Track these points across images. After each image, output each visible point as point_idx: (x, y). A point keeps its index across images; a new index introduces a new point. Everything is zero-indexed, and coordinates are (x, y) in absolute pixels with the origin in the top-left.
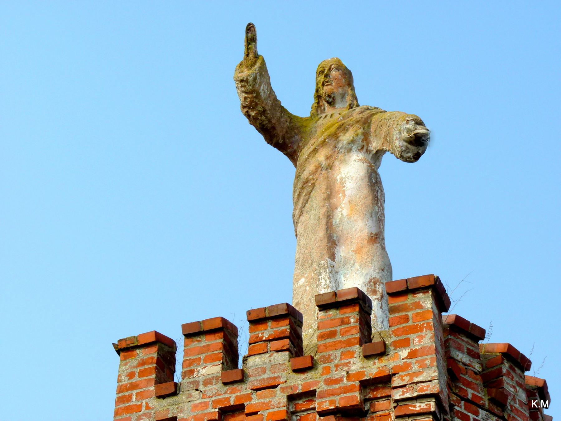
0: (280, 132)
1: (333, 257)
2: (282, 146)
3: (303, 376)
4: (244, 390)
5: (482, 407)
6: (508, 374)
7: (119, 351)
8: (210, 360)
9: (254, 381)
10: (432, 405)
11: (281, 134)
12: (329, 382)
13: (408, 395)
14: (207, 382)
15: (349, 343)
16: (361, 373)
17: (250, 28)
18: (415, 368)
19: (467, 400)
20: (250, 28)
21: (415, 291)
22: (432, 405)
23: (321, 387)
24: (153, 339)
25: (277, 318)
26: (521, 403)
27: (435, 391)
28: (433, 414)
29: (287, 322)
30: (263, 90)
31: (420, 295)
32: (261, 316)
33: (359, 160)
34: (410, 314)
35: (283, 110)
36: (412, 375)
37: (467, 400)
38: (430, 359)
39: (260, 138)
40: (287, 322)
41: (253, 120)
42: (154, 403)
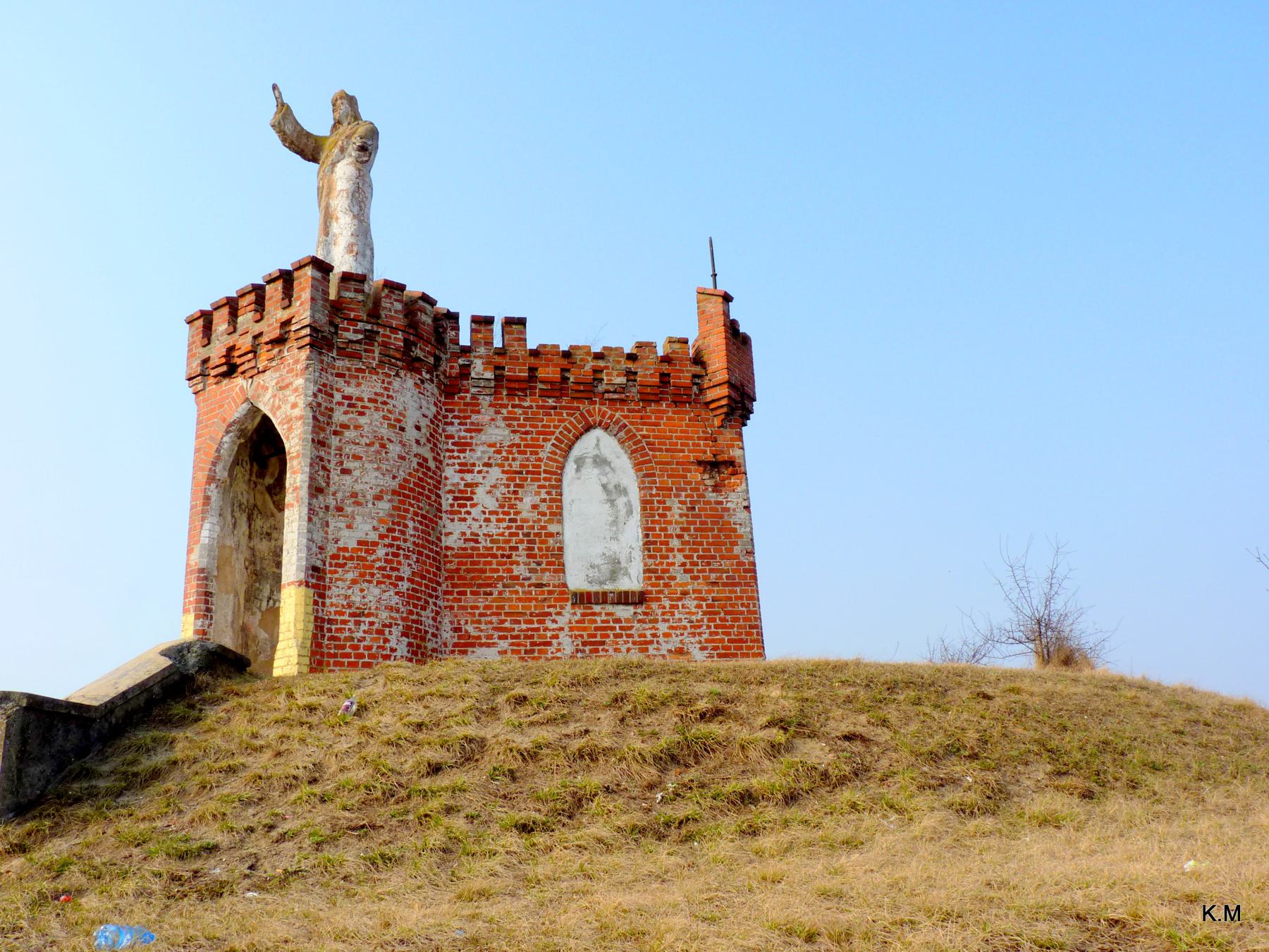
0: (308, 152)
1: (327, 234)
2: (314, 159)
3: (259, 324)
4: (236, 336)
5: (361, 321)
6: (387, 296)
7: (188, 323)
8: (223, 322)
9: (240, 330)
10: (307, 331)
11: (309, 153)
12: (269, 325)
13: (298, 328)
14: (222, 335)
15: (277, 302)
16: (281, 319)
17: (275, 87)
18: (301, 311)
19: (349, 320)
20: (275, 87)
21: (305, 266)
22: (307, 331)
23: (265, 329)
24: (199, 314)
25: (249, 292)
26: (396, 312)
27: (308, 323)
28: (310, 335)
29: (254, 294)
30: (288, 128)
31: (307, 268)
32: (242, 293)
33: (351, 163)
34: (302, 280)
35: (309, 135)
36: (302, 315)
37: (349, 320)
38: (308, 306)
39: (298, 157)
40: (254, 294)
41: (289, 148)
42: (201, 350)
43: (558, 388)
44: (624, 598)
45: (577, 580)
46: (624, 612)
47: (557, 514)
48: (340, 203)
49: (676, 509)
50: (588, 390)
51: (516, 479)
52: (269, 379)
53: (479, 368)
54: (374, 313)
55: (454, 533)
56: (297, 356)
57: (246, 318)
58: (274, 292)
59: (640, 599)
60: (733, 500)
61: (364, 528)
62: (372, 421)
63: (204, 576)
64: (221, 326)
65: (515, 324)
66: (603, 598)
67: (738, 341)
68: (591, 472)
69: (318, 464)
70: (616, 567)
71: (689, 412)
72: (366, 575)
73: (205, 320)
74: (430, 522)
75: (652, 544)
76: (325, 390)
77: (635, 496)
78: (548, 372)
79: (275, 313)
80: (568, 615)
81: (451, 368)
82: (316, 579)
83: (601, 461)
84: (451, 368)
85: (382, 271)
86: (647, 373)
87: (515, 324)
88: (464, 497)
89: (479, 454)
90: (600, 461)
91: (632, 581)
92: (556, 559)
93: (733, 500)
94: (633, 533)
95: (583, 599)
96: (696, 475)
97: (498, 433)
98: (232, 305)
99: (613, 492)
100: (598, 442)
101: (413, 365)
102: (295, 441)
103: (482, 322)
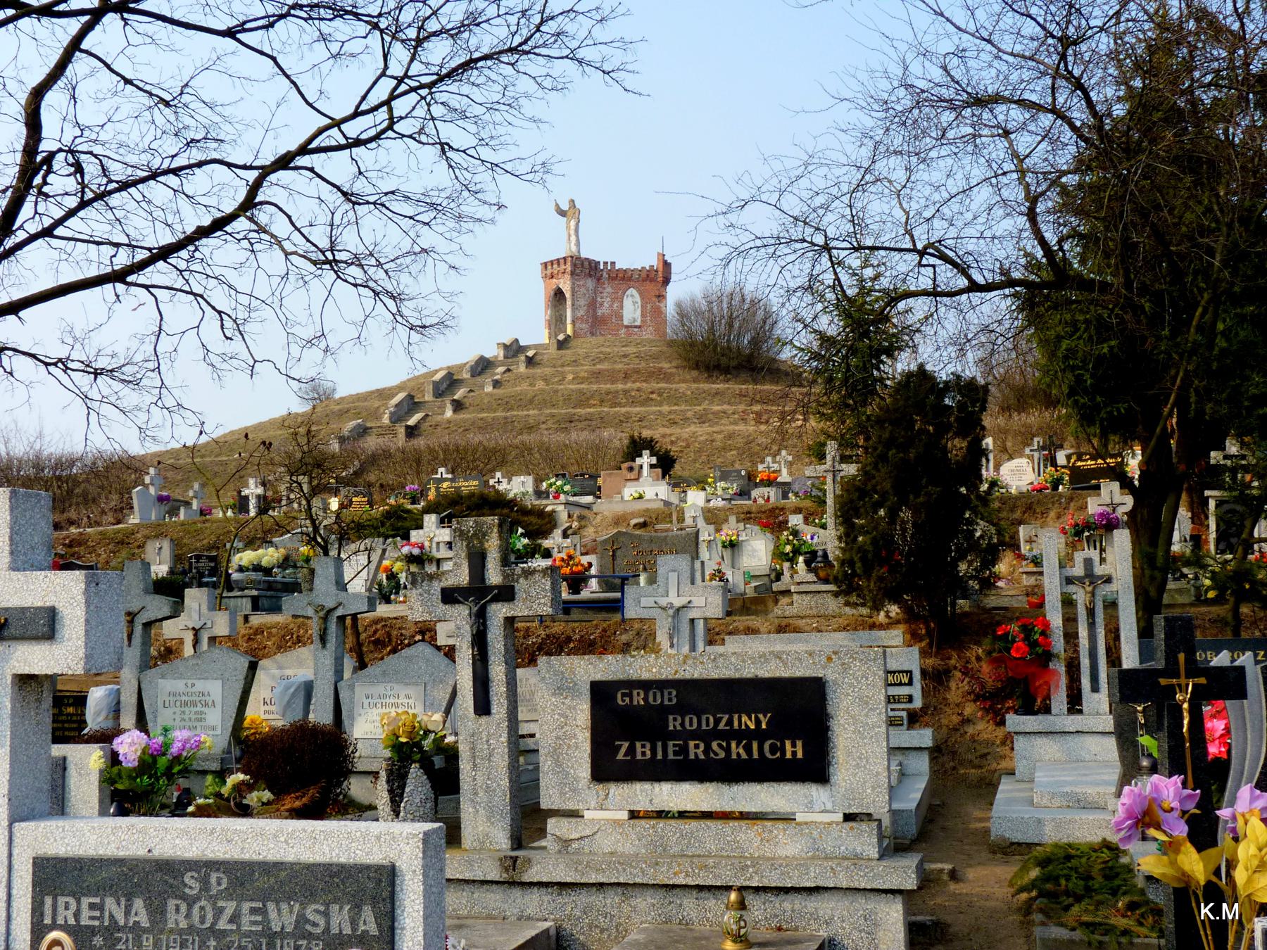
43: (623, 279)
44: (636, 327)
45: (626, 323)
46: (636, 330)
47: (622, 308)
48: (572, 232)
49: (649, 307)
50: (630, 279)
51: (613, 300)
52: (562, 281)
53: (605, 275)
54: (582, 265)
55: (599, 312)
56: (568, 277)
57: (555, 266)
58: (562, 261)
59: (639, 327)
60: (662, 305)
61: (582, 313)
62: (583, 290)
63: (549, 321)
64: (549, 267)
65: (613, 263)
66: (631, 327)
67: (667, 265)
68: (630, 298)
69: (573, 300)
70: (635, 320)
71: (653, 284)
72: (582, 322)
73: (545, 265)
74: (594, 310)
75: (643, 315)
76: (573, 284)
77: (640, 303)
78: (621, 275)
79: (563, 267)
80: (624, 330)
81: (598, 275)
82: (573, 323)
83: (632, 296)
84: (598, 275)
85: (583, 255)
86: (644, 275)
87: (613, 263)
88: (602, 304)
89: (605, 294)
90: (632, 296)
91: (638, 323)
92: (621, 318)
93: (662, 305)
94: (639, 312)
95: (627, 327)
96: (654, 299)
97: (609, 290)
98: (552, 262)
99: (635, 303)
100: (632, 291)
101: (590, 276)
102: (568, 295)
103: (606, 263)
